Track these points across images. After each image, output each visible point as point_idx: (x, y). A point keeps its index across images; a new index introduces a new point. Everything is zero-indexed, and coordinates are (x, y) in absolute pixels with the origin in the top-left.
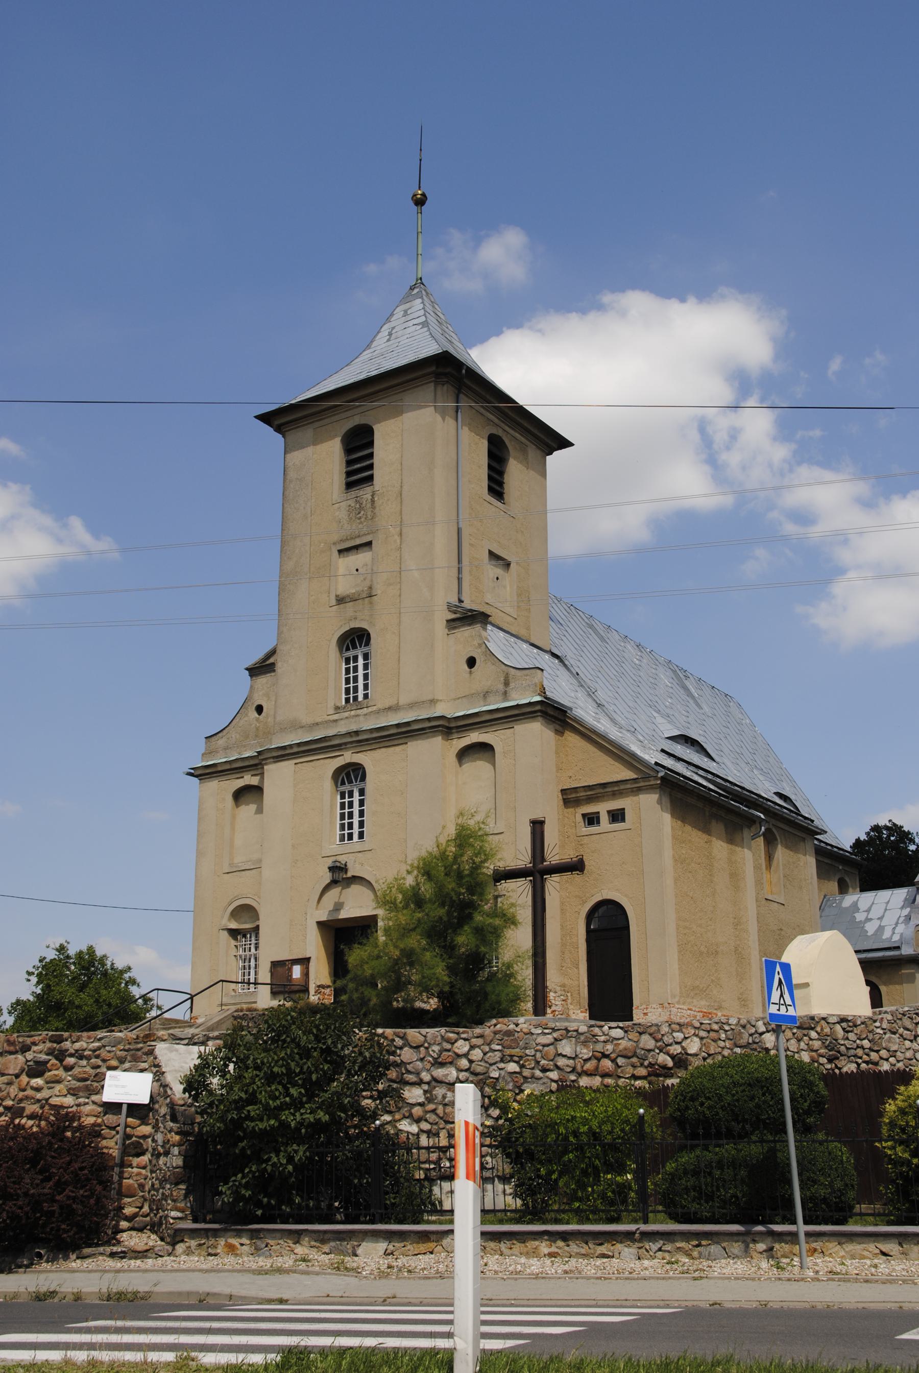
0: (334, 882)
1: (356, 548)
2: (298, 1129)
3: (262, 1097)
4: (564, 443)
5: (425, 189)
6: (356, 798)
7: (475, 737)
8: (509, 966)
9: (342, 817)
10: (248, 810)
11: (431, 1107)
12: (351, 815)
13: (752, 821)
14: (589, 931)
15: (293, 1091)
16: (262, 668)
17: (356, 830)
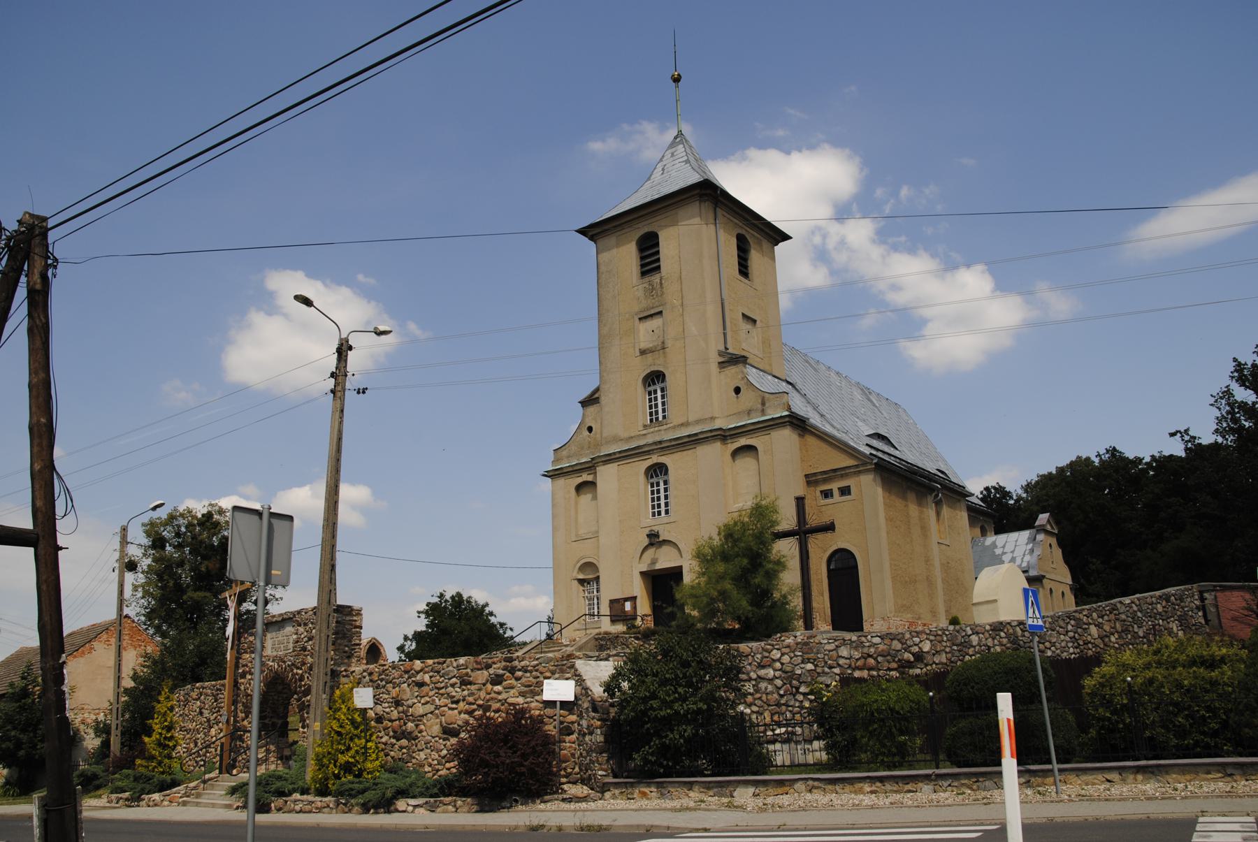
0: (651, 544)
1: (651, 316)
2: (685, 715)
3: (661, 694)
4: (786, 237)
5: (679, 71)
6: (662, 487)
7: (743, 441)
8: (785, 597)
9: (653, 500)
10: (586, 498)
11: (758, 695)
12: (659, 499)
13: (932, 490)
14: (829, 570)
15: (680, 690)
16: (590, 401)
17: (663, 508)
